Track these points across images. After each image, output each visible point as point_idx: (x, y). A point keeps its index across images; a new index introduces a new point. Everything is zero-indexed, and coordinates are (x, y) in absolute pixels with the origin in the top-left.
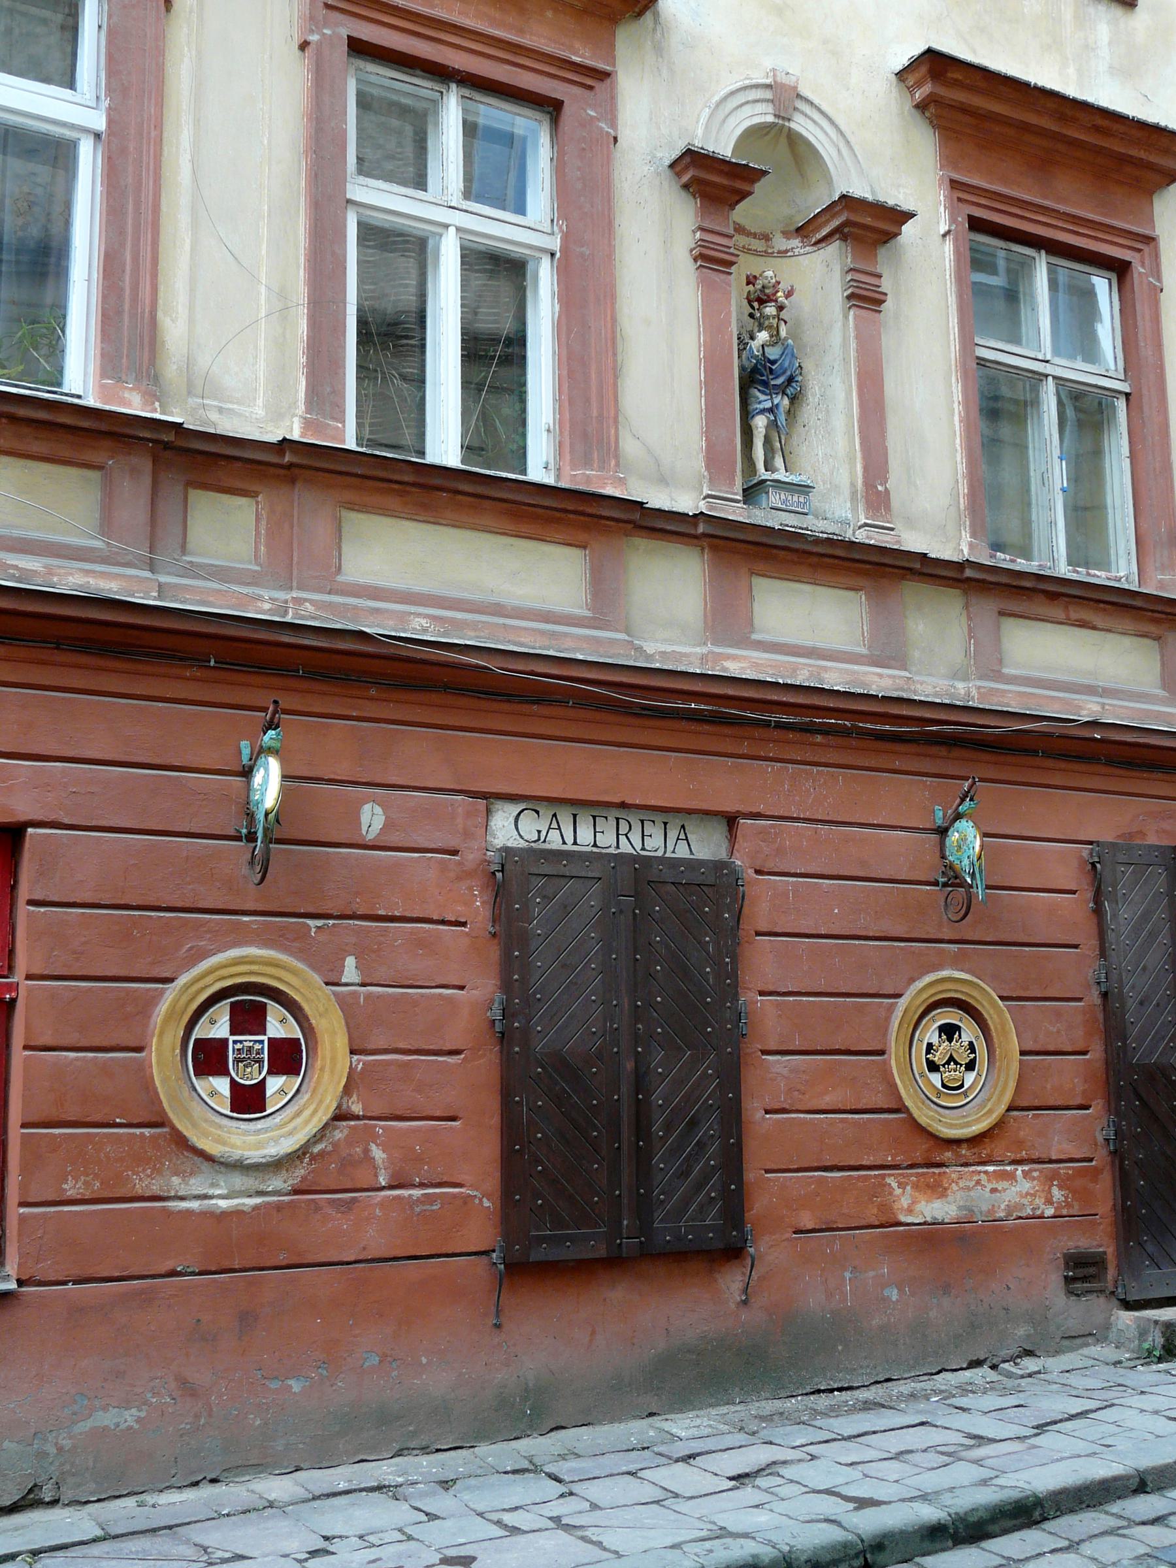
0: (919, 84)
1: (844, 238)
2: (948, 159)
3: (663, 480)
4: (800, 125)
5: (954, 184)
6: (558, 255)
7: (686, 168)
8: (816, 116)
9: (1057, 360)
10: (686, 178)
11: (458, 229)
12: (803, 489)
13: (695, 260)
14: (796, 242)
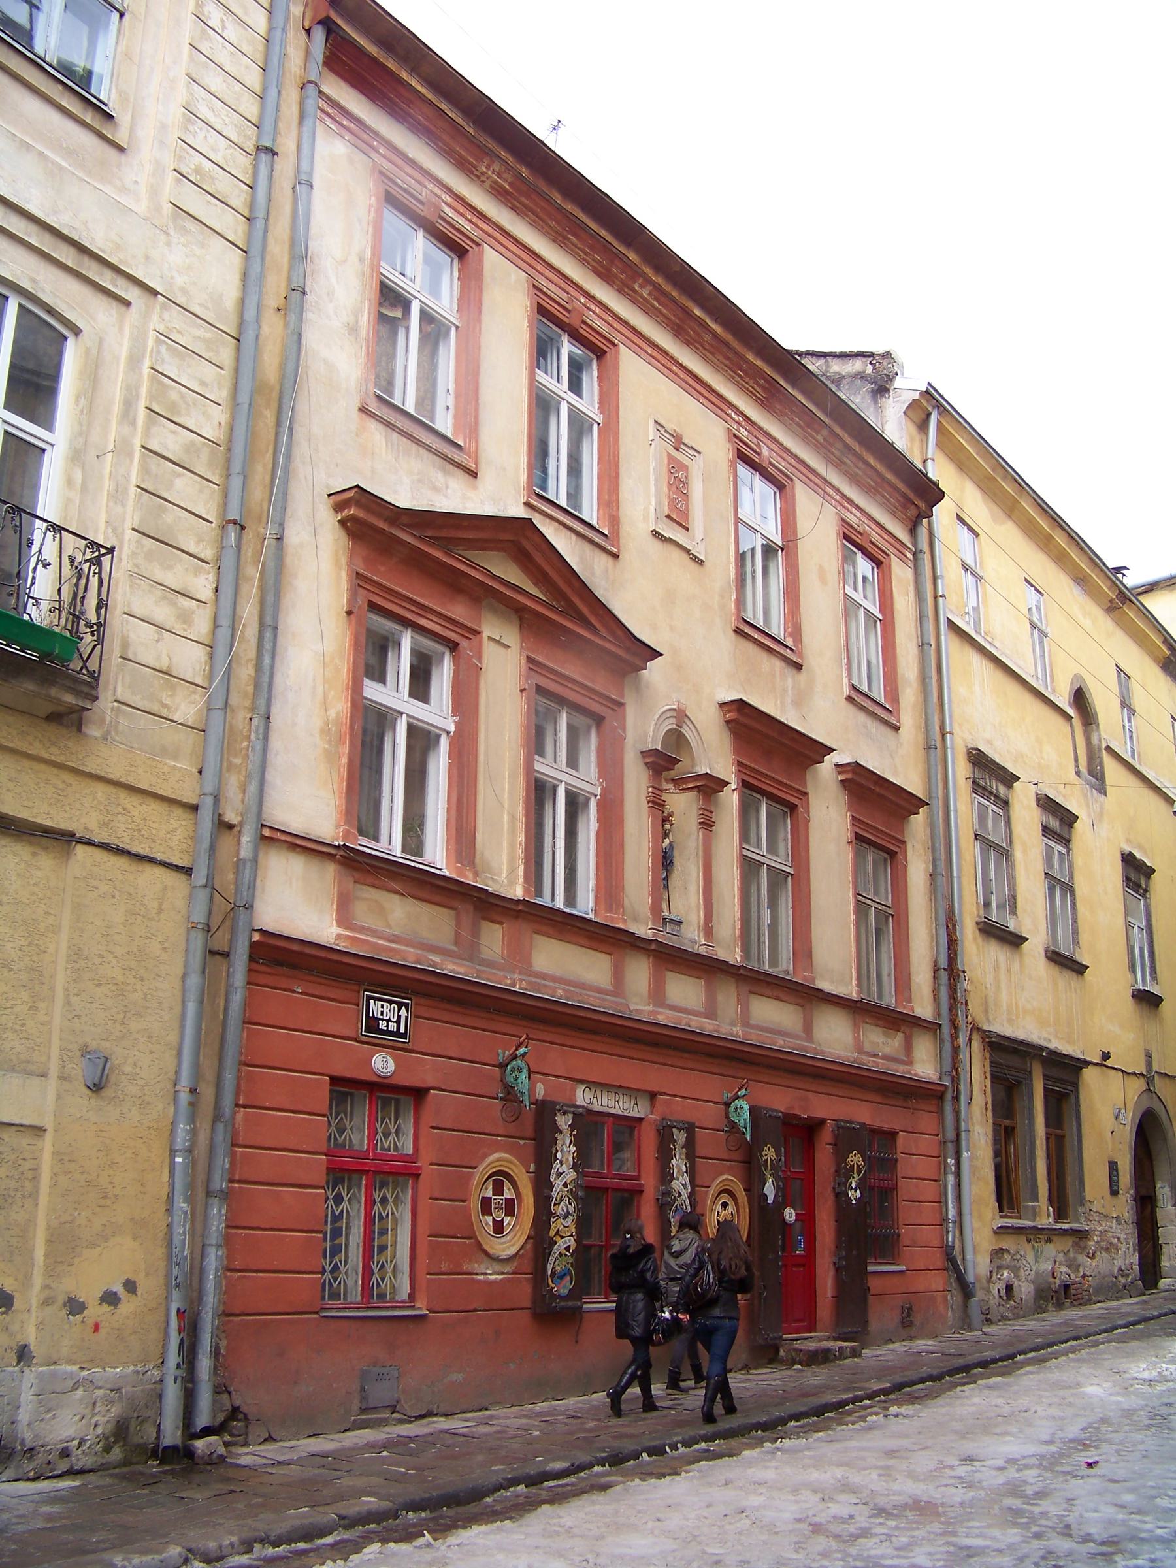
0: (730, 712)
1: (699, 792)
2: (737, 751)
3: (636, 919)
4: (685, 730)
5: (739, 764)
6: (598, 797)
7: (651, 756)
8: (691, 725)
9: (769, 856)
10: (648, 760)
11: (566, 783)
12: (678, 923)
13: (649, 802)
14: (671, 786)
